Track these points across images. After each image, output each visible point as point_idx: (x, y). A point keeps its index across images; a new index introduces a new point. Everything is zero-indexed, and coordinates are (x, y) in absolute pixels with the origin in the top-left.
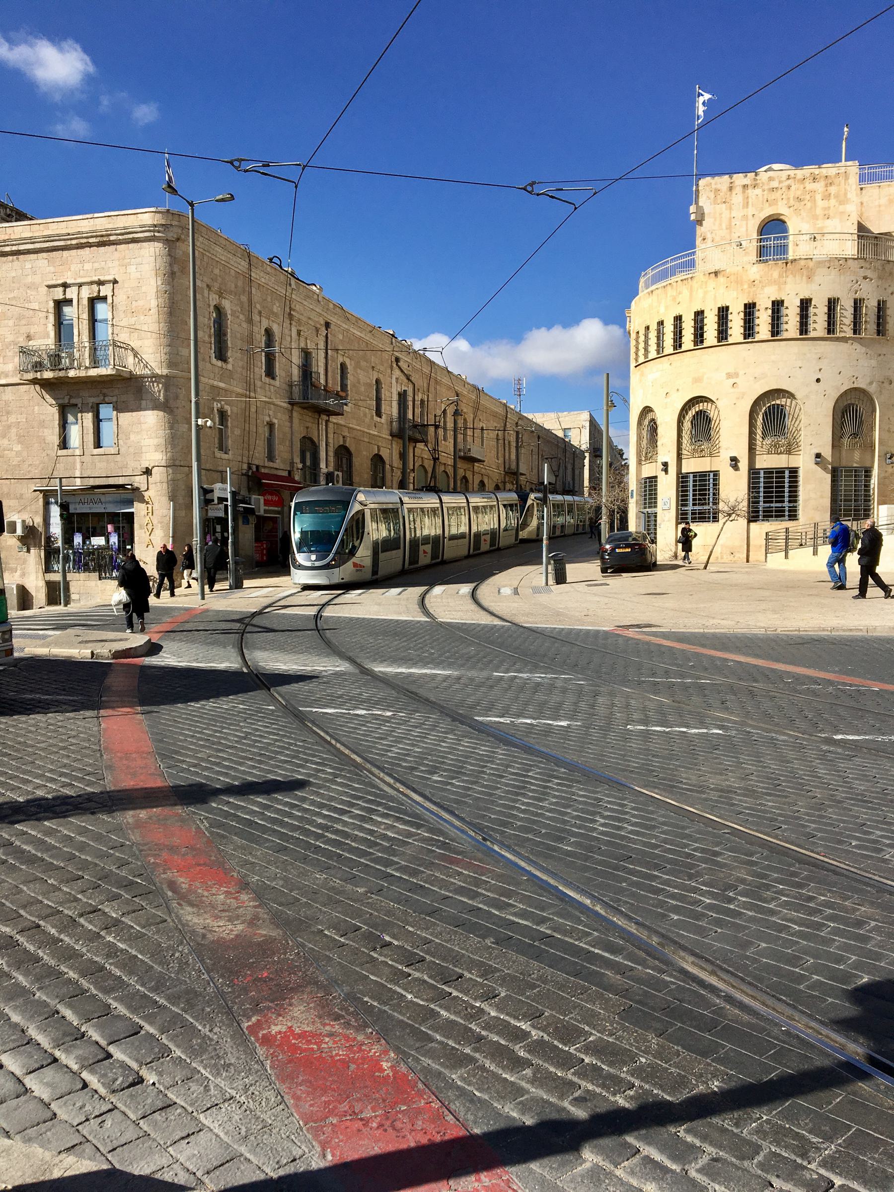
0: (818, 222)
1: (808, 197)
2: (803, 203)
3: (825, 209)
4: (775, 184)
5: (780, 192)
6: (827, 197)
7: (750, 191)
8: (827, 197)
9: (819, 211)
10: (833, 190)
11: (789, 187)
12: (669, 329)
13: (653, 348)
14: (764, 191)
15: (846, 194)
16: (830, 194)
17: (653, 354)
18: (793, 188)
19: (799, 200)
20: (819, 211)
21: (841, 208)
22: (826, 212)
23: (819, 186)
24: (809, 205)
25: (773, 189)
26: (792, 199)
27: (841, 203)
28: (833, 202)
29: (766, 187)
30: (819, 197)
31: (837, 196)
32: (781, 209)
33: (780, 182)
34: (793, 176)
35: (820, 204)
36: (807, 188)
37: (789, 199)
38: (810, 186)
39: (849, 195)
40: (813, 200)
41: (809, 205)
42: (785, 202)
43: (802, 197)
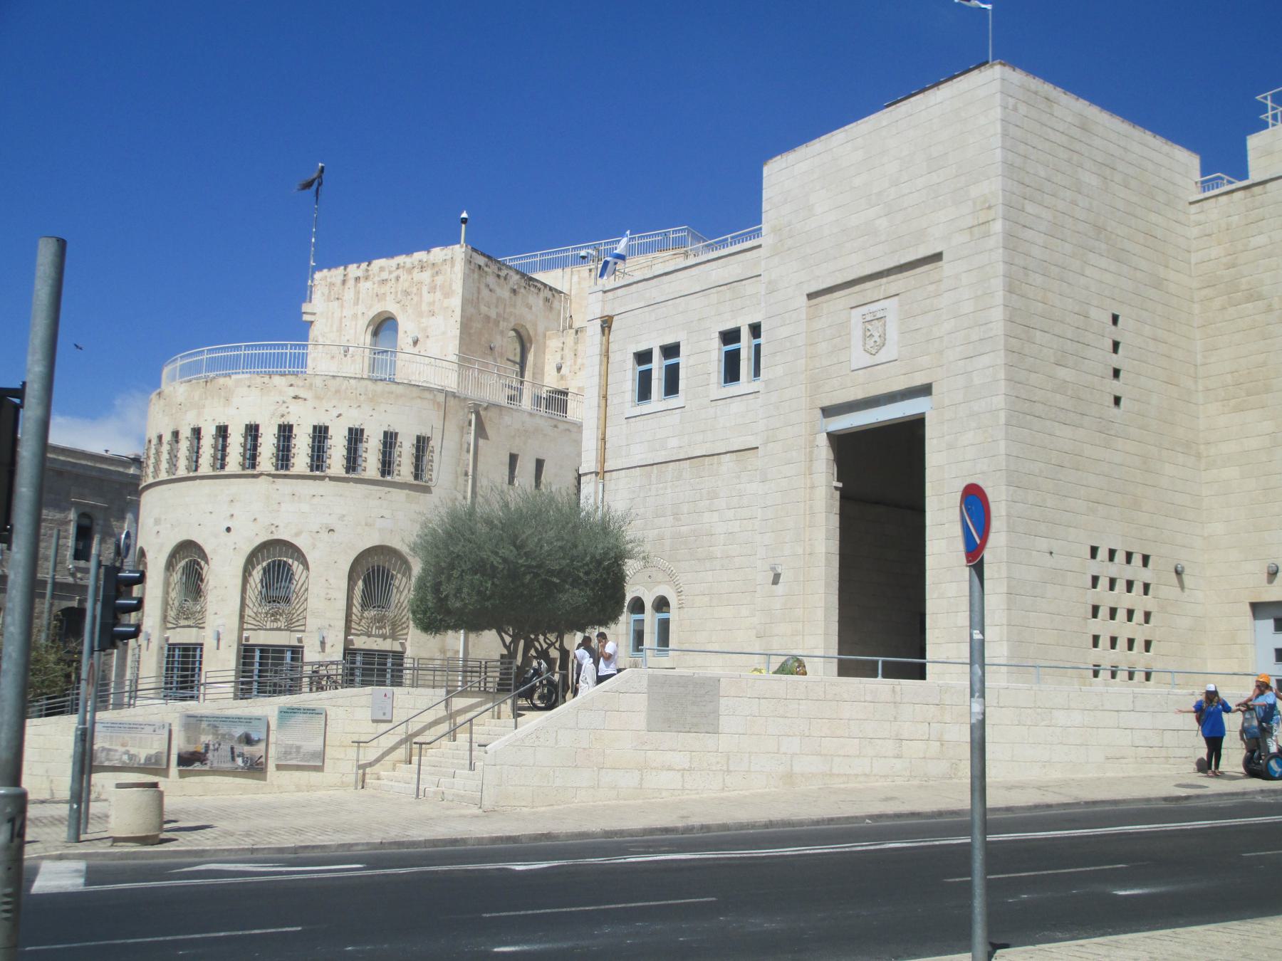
0: (424, 320)
1: (414, 290)
2: (409, 297)
4: (385, 275)
5: (389, 284)
6: (432, 289)
8: (432, 289)
9: (425, 307)
11: (398, 278)
12: (236, 440)
13: (164, 465)
14: (374, 284)
16: (436, 285)
18: (401, 280)
19: (407, 293)
20: (425, 307)
23: (426, 276)
24: (416, 299)
25: (384, 281)
29: (377, 279)
30: (425, 290)
32: (391, 307)
33: (390, 272)
34: (402, 264)
35: (427, 297)
37: (397, 292)
38: (417, 275)
41: (416, 299)
42: (393, 296)
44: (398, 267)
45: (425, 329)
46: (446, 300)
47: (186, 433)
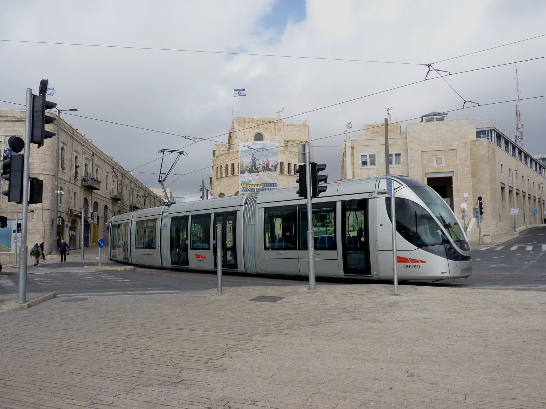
1: (269, 128)
2: (267, 130)
3: (274, 132)
7: (251, 124)
10: (277, 127)
15: (280, 129)
16: (276, 128)
17: (224, 175)
21: (279, 133)
22: (275, 133)
24: (269, 130)
26: (264, 128)
27: (279, 131)
28: (277, 130)
29: (256, 123)
30: (272, 128)
31: (277, 129)
32: (261, 131)
33: (260, 122)
34: (264, 121)
36: (269, 125)
39: (282, 129)
40: (270, 129)
42: (262, 128)
43: (267, 128)
44: (263, 121)
45: (274, 138)
46: (279, 132)
47: (224, 166)
